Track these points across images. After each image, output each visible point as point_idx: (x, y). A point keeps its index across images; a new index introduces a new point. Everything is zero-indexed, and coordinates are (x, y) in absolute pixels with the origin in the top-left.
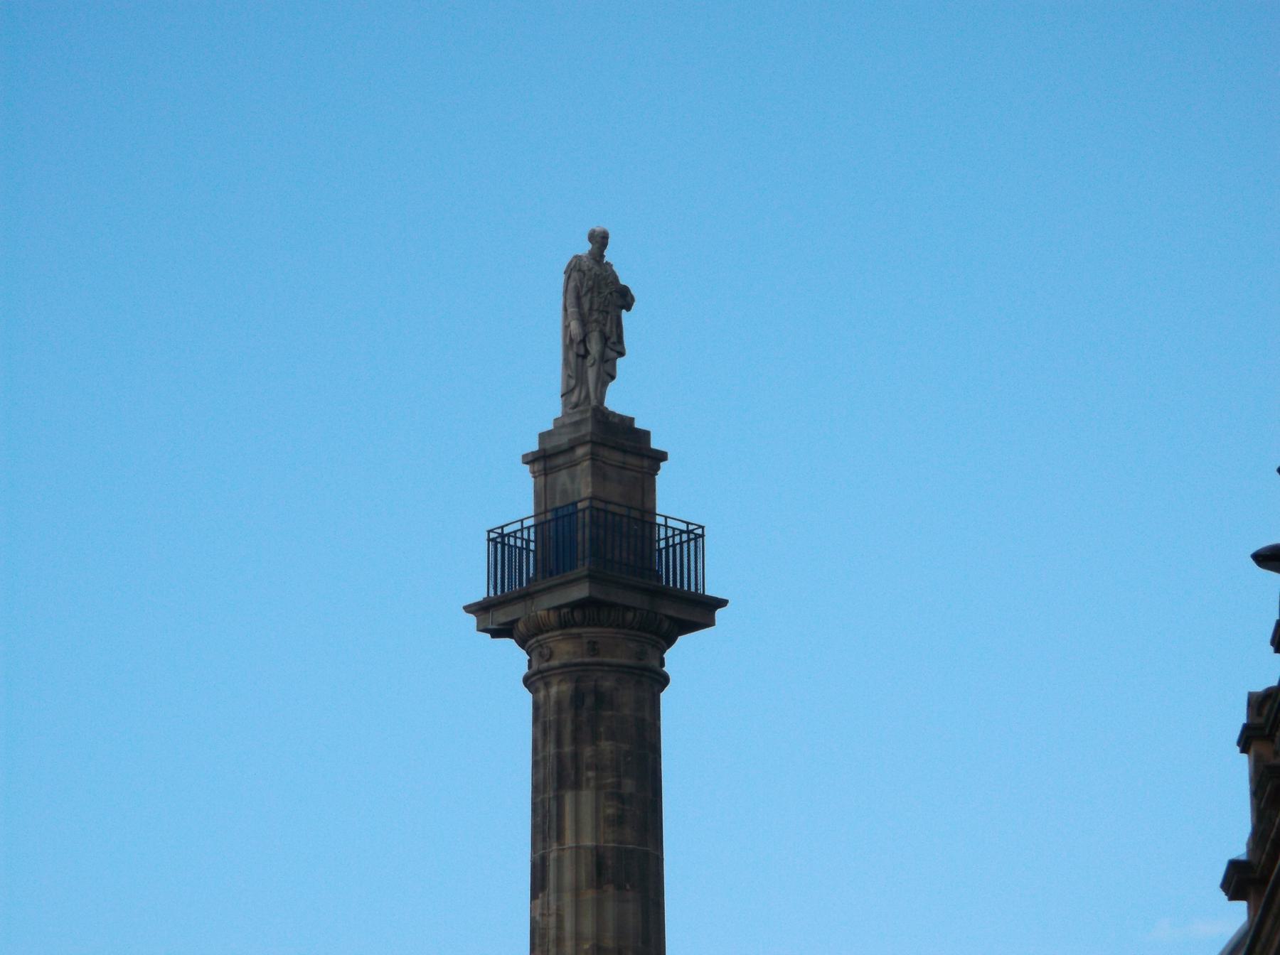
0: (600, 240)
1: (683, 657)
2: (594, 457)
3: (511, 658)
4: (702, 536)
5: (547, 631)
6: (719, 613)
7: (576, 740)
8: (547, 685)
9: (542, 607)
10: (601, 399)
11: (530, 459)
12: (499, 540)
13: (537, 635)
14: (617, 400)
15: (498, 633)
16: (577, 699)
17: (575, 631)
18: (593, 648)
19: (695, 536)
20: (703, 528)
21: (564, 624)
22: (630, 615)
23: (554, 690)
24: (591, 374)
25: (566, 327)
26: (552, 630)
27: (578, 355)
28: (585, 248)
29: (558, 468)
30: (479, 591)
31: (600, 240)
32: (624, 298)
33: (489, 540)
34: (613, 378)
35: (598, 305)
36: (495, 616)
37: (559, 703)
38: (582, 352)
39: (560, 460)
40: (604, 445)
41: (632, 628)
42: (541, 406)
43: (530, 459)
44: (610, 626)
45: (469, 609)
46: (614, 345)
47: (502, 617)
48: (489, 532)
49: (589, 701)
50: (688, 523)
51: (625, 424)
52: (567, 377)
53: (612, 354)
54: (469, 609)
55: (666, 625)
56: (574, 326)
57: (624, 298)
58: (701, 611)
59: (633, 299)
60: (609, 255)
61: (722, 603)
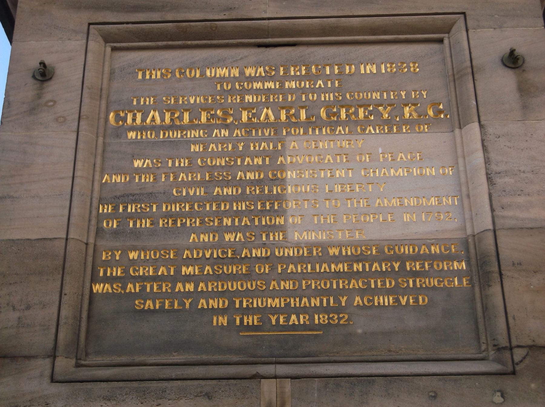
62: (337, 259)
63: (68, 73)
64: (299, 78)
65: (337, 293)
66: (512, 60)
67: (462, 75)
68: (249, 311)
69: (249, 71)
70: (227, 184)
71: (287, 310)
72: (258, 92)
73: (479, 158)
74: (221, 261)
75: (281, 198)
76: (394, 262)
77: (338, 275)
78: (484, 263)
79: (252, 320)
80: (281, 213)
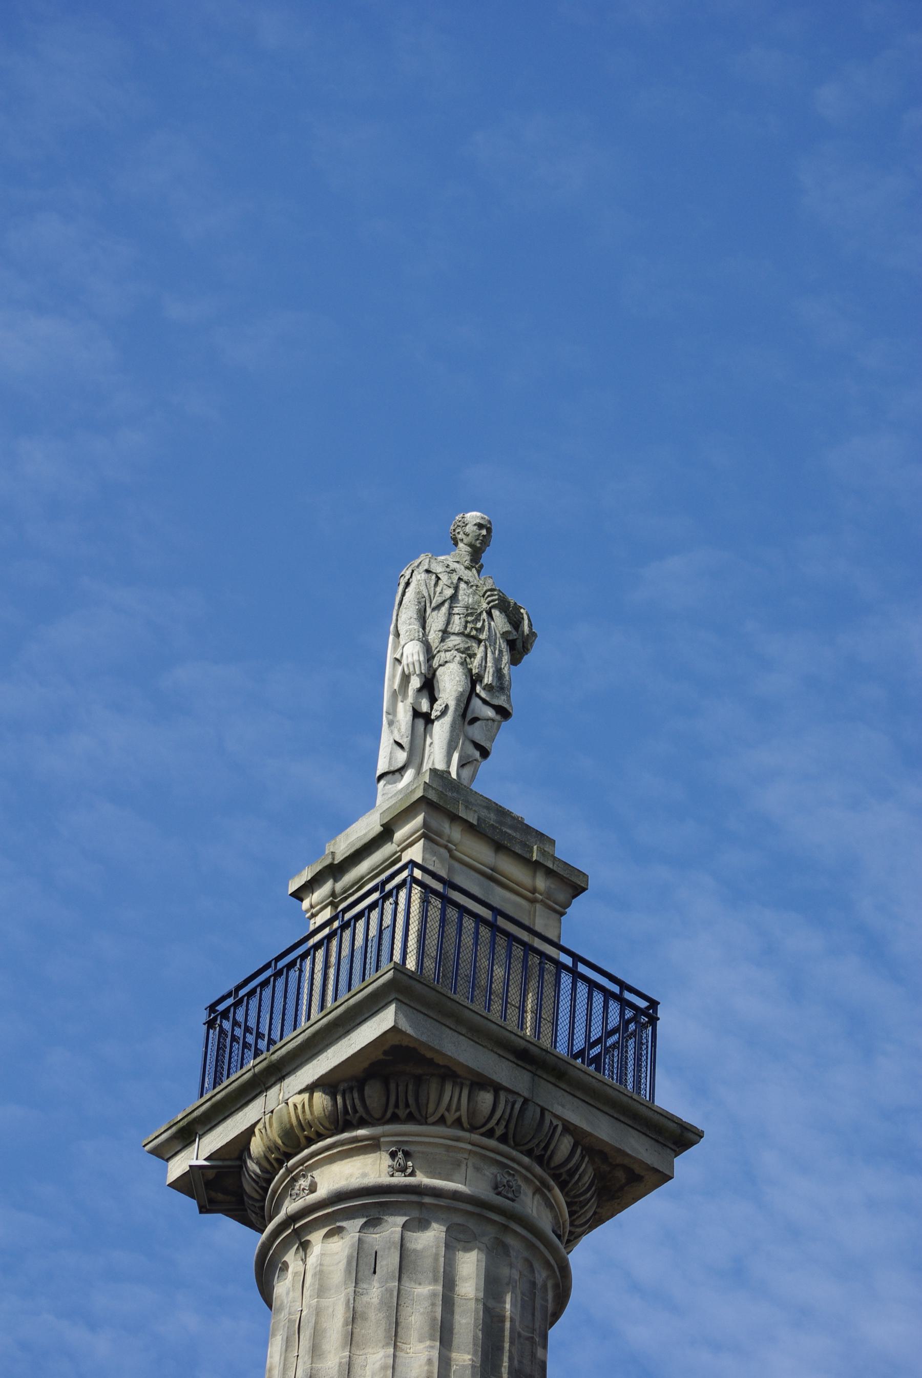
2: (428, 835)
4: (653, 1020)
5: (310, 1141)
7: (351, 1340)
13: (289, 1156)
16: (362, 1265)
18: (403, 1155)
20: (654, 1004)
21: (340, 1122)
22: (486, 1099)
26: (320, 1137)
27: (416, 714)
33: (210, 1024)
37: (320, 1274)
38: (425, 706)
40: (454, 818)
41: (490, 1134)
44: (442, 1121)
48: (212, 1008)
49: (390, 1262)
55: (565, 1144)
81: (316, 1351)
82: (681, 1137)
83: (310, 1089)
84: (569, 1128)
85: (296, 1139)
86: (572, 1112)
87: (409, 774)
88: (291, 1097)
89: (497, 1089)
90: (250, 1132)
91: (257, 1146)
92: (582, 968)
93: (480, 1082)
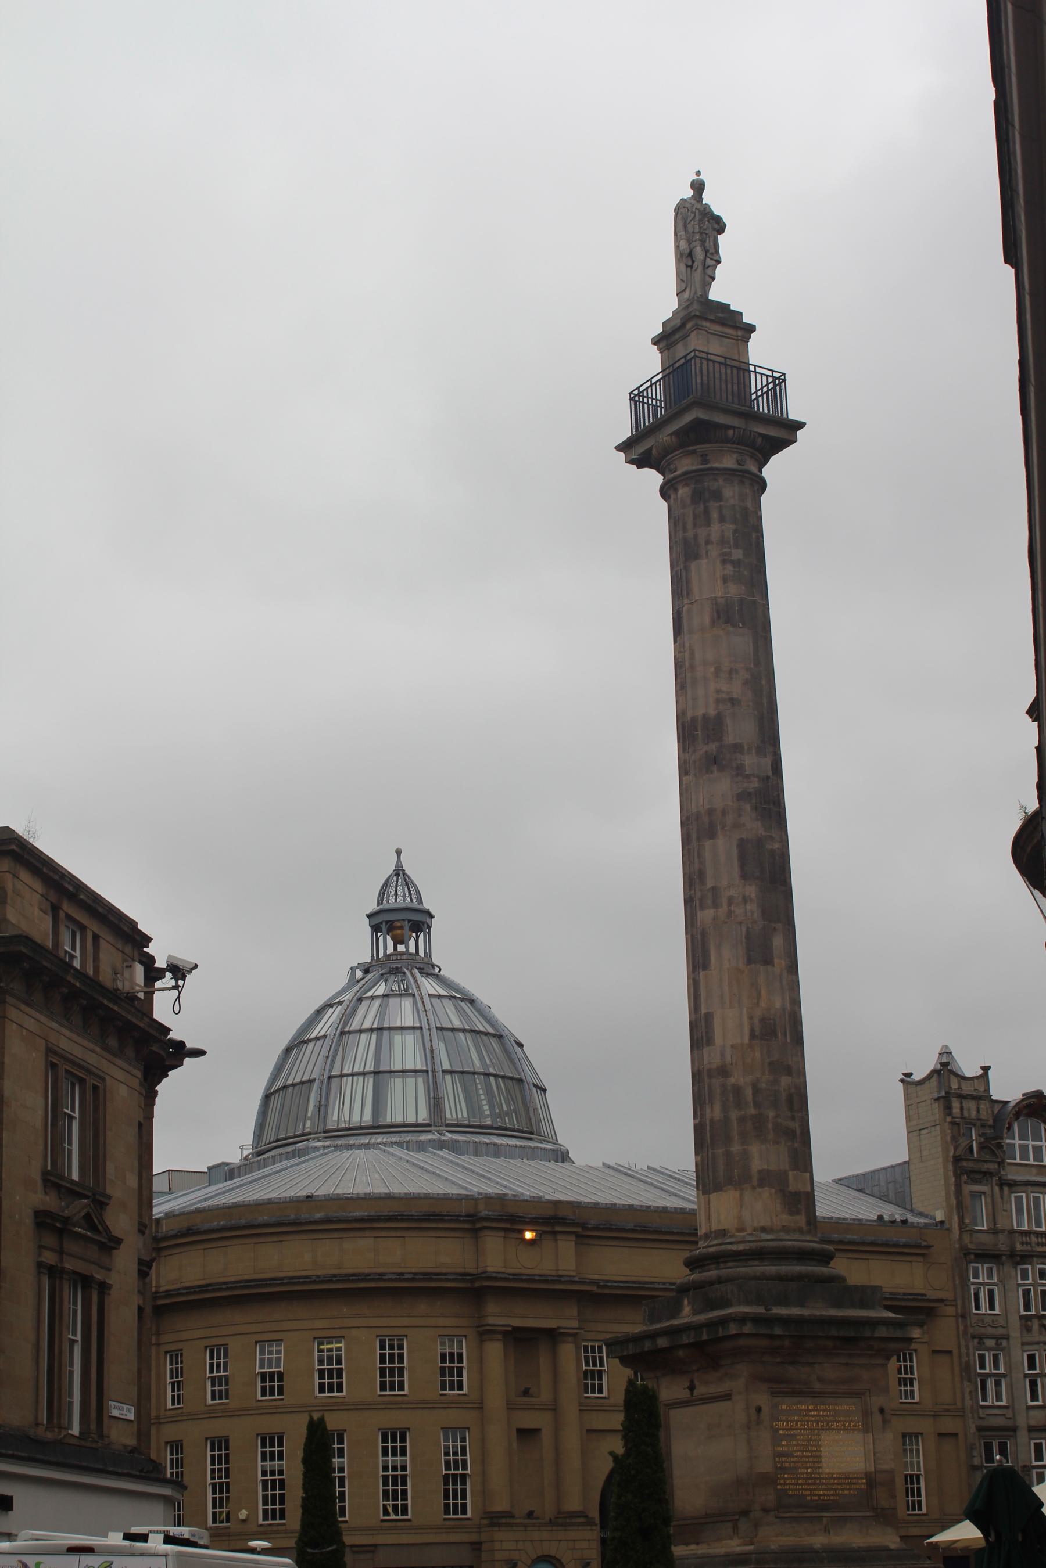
0: (698, 187)
1: (777, 469)
3: (653, 478)
4: (784, 380)
6: (800, 433)
8: (676, 490)
9: (665, 437)
10: (706, 294)
11: (657, 341)
12: (636, 399)
14: (717, 293)
15: (641, 462)
17: (691, 448)
19: (779, 381)
20: (784, 374)
22: (730, 432)
23: (680, 492)
24: (698, 275)
25: (677, 247)
26: (676, 450)
27: (687, 266)
28: (689, 193)
29: (676, 343)
30: (625, 432)
31: (698, 187)
32: (719, 226)
33: (631, 399)
34: (713, 279)
35: (698, 231)
36: (639, 450)
38: (690, 263)
39: (677, 336)
40: (706, 319)
41: (733, 443)
42: (664, 303)
43: (657, 341)
44: (716, 442)
45: (619, 448)
46: (713, 257)
47: (641, 449)
48: (631, 393)
50: (773, 371)
51: (725, 307)
52: (680, 280)
53: (709, 262)
54: (619, 448)
55: (759, 440)
56: (683, 244)
57: (719, 226)
58: (783, 432)
59: (725, 225)
60: (707, 198)
61: (800, 425)
62: (834, 1479)
63: (766, 1410)
64: (824, 1411)
65: (836, 1490)
66: (882, 1411)
67: (866, 1414)
68: (815, 1495)
69: (811, 1407)
70: (806, 1451)
71: (824, 1495)
72: (813, 1416)
73: (871, 1446)
74: (807, 1479)
75: (820, 1457)
76: (847, 1478)
77: (834, 1484)
78: (871, 1480)
79: (816, 1498)
80: (820, 1462)
81: (685, 530)
82: (800, 425)
83: (671, 435)
84: (760, 434)
85: (667, 451)
86: (761, 429)
87: (688, 291)
88: (665, 437)
89: (734, 428)
90: (650, 449)
91: (654, 452)
92: (758, 370)
93: (728, 427)
